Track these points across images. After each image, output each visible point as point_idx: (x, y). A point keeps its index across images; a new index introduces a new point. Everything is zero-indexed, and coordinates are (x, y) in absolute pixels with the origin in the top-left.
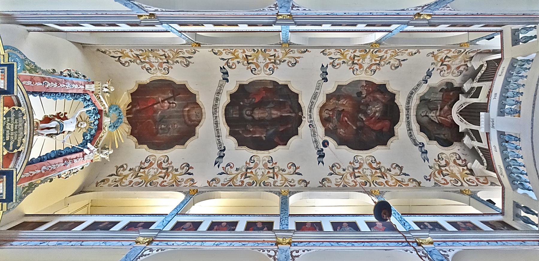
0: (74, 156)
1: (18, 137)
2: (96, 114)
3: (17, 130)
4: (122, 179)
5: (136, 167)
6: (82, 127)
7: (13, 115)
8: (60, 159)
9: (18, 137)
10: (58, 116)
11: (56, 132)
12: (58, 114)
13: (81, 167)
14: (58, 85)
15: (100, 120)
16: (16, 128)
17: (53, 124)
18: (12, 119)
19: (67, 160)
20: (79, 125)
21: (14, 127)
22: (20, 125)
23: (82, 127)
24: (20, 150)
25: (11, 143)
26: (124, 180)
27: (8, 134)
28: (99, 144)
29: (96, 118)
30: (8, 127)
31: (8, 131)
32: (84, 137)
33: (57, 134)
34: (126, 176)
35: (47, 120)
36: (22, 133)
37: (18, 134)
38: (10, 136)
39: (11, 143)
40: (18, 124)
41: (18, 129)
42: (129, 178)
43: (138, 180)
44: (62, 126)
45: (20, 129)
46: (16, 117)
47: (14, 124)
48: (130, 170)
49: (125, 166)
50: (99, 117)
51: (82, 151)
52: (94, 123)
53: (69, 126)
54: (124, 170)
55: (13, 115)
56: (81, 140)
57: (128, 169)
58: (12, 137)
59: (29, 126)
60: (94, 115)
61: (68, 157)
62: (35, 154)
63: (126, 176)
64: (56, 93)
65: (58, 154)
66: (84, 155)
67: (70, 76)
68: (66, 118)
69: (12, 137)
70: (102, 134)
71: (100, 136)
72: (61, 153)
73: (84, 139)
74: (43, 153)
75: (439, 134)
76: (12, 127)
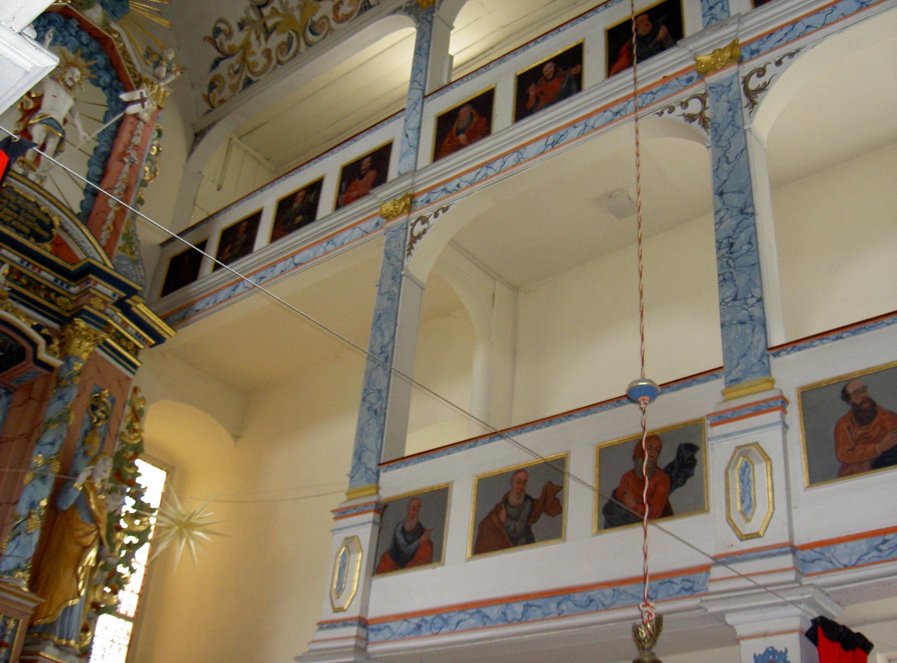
0: (125, 135)
1: (32, 214)
2: (66, 26)
3: (20, 208)
4: (244, 59)
5: (246, 12)
6: (76, 80)
8: (114, 164)
9: (32, 214)
11: (57, 140)
12: (22, 109)
13: (156, 134)
15: (84, 26)
16: (16, 208)
19: (124, 154)
20: (70, 83)
21: (10, 208)
22: (13, 198)
23: (76, 80)
24: (57, 224)
25: (38, 229)
26: (251, 59)
27: (20, 226)
28: (135, 69)
29: (73, 31)
30: (7, 219)
31: (14, 223)
32: (98, 85)
33: (62, 140)
34: (246, 47)
36: (29, 205)
37: (26, 211)
38: (23, 224)
39: (38, 229)
40: (9, 201)
41: (17, 205)
42: (258, 48)
43: (276, 39)
44: (50, 122)
45: (20, 202)
47: (7, 206)
48: (241, 26)
49: (223, 26)
50: (74, 23)
51: (125, 116)
52: (82, 44)
54: (229, 35)
56: (102, 97)
57: (235, 28)
58: (29, 223)
59: (23, 186)
60: (66, 33)
61: (120, 148)
62: (75, 199)
63: (246, 47)
66: (136, 116)
68: (38, 101)
69: (29, 223)
70: (118, 47)
71: (120, 52)
72: (104, 153)
73: (104, 89)
76: (10, 212)
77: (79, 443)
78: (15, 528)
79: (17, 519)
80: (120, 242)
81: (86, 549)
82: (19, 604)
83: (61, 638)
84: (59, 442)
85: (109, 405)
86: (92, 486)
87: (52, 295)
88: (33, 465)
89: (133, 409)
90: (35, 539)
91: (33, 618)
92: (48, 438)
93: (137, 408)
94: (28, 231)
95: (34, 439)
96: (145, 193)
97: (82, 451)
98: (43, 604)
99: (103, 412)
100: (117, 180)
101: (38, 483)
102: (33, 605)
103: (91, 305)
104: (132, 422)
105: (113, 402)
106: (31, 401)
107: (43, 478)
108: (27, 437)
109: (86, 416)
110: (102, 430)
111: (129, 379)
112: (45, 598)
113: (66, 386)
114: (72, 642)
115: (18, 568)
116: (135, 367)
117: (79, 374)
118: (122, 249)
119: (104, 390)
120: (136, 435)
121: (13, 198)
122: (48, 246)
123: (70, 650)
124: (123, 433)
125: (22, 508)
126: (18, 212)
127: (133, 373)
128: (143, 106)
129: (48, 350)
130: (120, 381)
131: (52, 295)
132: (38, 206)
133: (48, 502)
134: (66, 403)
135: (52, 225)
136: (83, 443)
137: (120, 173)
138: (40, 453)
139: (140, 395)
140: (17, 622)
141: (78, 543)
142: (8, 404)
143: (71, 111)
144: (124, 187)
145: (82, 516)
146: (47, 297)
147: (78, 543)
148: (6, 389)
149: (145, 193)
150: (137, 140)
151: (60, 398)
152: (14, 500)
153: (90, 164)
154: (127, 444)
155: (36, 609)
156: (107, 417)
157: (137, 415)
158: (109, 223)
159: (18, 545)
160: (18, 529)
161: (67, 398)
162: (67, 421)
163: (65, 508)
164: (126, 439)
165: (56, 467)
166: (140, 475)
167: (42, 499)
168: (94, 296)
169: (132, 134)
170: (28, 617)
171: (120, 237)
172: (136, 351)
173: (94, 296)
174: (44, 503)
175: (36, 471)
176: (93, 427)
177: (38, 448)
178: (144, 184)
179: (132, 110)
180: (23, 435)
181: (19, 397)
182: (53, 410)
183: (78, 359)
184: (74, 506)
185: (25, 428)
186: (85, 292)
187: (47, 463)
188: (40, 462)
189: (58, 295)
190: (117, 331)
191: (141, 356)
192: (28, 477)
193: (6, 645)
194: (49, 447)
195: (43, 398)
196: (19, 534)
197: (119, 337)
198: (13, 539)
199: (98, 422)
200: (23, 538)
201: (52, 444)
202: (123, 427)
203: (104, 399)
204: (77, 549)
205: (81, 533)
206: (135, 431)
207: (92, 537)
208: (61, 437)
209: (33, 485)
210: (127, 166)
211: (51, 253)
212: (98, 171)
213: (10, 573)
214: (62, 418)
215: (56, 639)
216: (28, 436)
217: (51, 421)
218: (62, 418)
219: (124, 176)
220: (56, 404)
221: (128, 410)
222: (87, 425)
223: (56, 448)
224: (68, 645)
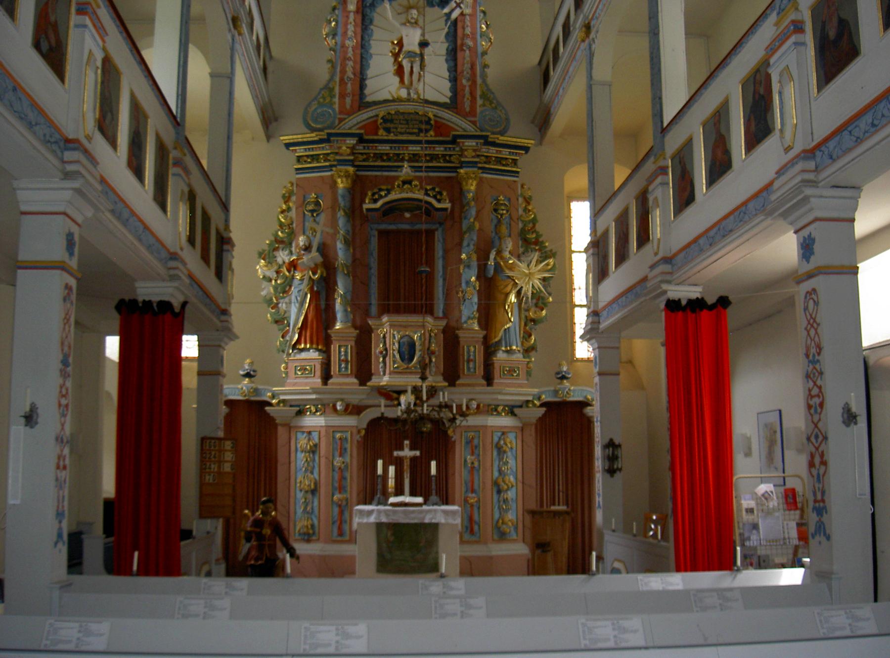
0: (460, 31)
3: (407, 120)
7: (388, 125)
10: (396, 56)
13: (482, 15)
14: (349, 59)
17: (406, 64)
18: (392, 126)
19: (462, 45)
20: (413, 21)
22: (401, 117)
24: (432, 117)
27: (411, 131)
30: (403, 130)
35: (400, 71)
36: (412, 116)
46: (391, 121)
53: (412, 39)
55: (388, 125)
61: (459, 42)
64: (362, 57)
65: (453, 54)
67: (334, 35)
68: (400, 44)
74: (446, 74)
75: (342, 96)
77: (494, 234)
80: (479, 102)
83: (506, 347)
87: (447, 158)
89: (525, 198)
94: (416, 131)
96: (488, 59)
100: (463, 64)
101: (466, 270)
103: (466, 157)
107: (469, 267)
111: (515, 181)
114: (514, 347)
116: (518, 172)
118: (484, 105)
121: (401, 117)
122: (432, 133)
126: (407, 124)
128: (461, 8)
129: (439, 201)
131: (447, 158)
132: (417, 113)
135: (430, 119)
136: (496, 233)
137: (464, 58)
140: (475, 347)
143: (423, 35)
144: (469, 66)
146: (445, 161)
149: (488, 59)
150: (468, 31)
153: (447, 61)
156: (507, 211)
157: (528, 201)
158: (467, 95)
163: (490, 276)
166: (541, 235)
168: (466, 150)
169: (464, 28)
171: (478, 98)
172: (515, 162)
173: (466, 150)
178: (485, 53)
179: (454, 15)
183: (469, 191)
186: (462, 150)
187: (469, 257)
189: (450, 156)
190: (496, 157)
191: (519, 163)
192: (462, 267)
197: (499, 160)
201: (468, 245)
202: (521, 211)
204: (503, 296)
208: (472, 240)
210: (467, 52)
211: (435, 136)
212: (452, 64)
213: (466, 322)
214: (470, 228)
215: (503, 349)
219: (468, 59)
221: (521, 200)
222: (495, 221)
224: (511, 350)
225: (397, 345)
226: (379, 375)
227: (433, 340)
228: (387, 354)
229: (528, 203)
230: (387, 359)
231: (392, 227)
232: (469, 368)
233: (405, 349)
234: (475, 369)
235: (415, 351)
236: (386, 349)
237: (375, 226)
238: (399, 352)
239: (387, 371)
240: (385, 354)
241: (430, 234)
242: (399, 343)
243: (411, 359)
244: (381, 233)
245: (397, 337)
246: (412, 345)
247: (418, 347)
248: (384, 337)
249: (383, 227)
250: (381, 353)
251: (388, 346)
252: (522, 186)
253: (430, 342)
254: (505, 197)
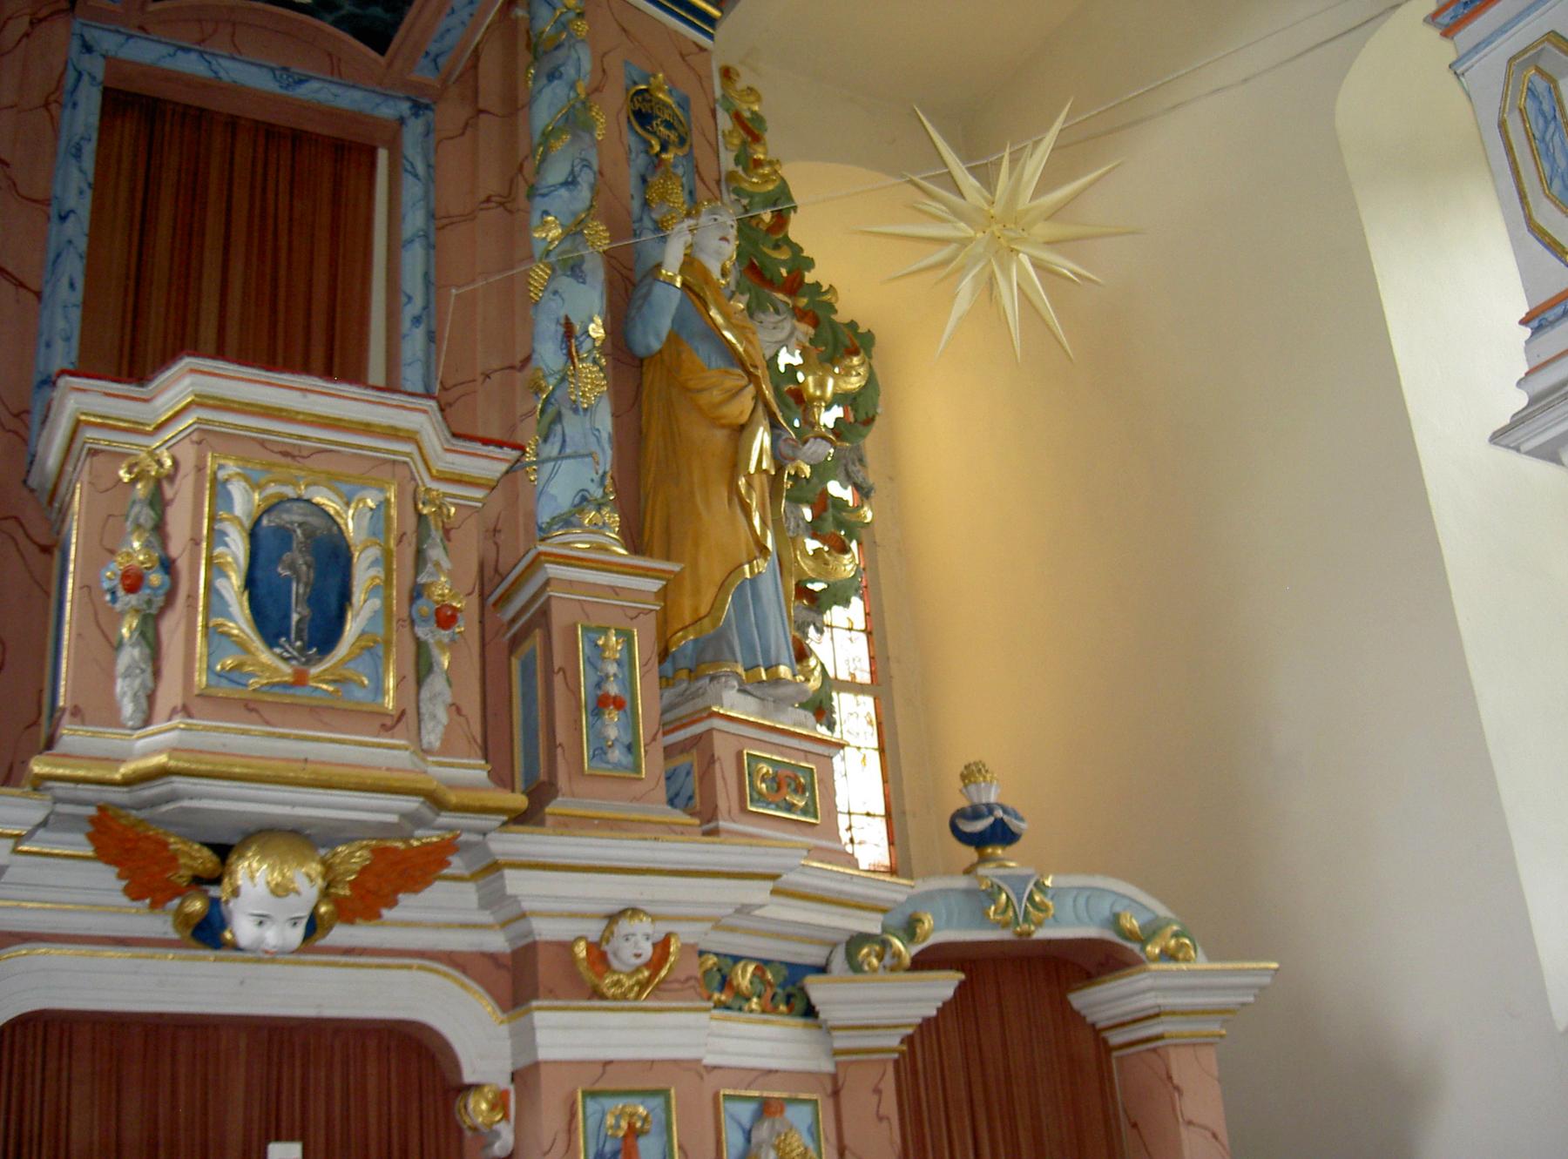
77: (636, 205)
78: (543, 411)
79: (538, 390)
81: (741, 432)
82: (615, 591)
84: (586, 178)
85: (678, 112)
86: (705, 274)
88: (539, 250)
89: (737, 117)
90: (605, 421)
91: (664, 620)
92: (556, 173)
93: (747, 114)
95: (522, 190)
97: (648, 223)
98: (677, 574)
99: (669, 125)
101: (565, 283)
102: (654, 585)
104: (744, 143)
105: (684, 104)
106: (482, 116)
107: (575, 269)
108: (501, 204)
109: (631, 140)
110: (680, 171)
111: (702, 49)
112: (679, 560)
113: (558, 47)
115: (583, 501)
116: (711, 21)
117: (580, 15)
119: (655, 76)
120: (766, 170)
123: (781, 691)
124: (731, 176)
125: (549, 355)
127: (711, 37)
130: (682, 56)
133: (604, 327)
134: (573, 86)
136: (646, 204)
138: (547, 213)
139: (741, 84)
141: (716, 422)
142: (427, 134)
145: (700, 356)
147: (716, 422)
148: (408, 99)
151: (553, 76)
152: (520, 357)
154: (751, 196)
155: (663, 594)
157: (751, 130)
159: (564, 441)
160: (551, 411)
161: (569, 71)
162: (589, 128)
163: (656, 346)
164: (745, 185)
165: (599, 237)
166: (809, 263)
167: (592, 321)
170: (651, 622)
174: (597, 330)
175: (552, 259)
176: (656, 163)
177: (540, 204)
180: (488, 200)
181: (452, 113)
182: (546, 107)
184: (674, 338)
185: (491, 184)
187: (574, 231)
188: (556, 232)
192: (540, 273)
193: (618, 704)
194: (563, 192)
195: (514, 106)
196: (558, 417)
198: (545, 440)
199: (664, 148)
200: (572, 426)
201: (571, 183)
202: (728, 161)
203: (661, 96)
204: (720, 436)
205: (716, 395)
206: (758, 164)
207: (746, 402)
209: (555, 293)
216: (506, 202)
217: (546, 136)
218: (575, 121)
220: (547, 94)
221: (725, 122)
222: (641, 161)
223: (584, 193)
224: (777, 681)
225: (236, 548)
226: (111, 717)
227: (436, 553)
228: (171, 596)
229: (757, 139)
230: (171, 627)
231: (190, 64)
232: (600, 752)
233: (295, 574)
234: (631, 748)
235: (345, 596)
236: (168, 566)
237: (108, 42)
238: (250, 583)
239: (170, 693)
240: (156, 591)
241: (347, 155)
242: (253, 535)
243: (325, 633)
244: (129, 105)
245: (243, 501)
246: (333, 557)
247: (364, 574)
248: (158, 502)
249: (145, 52)
250: (133, 581)
251: (177, 547)
252: (727, 73)
253: (420, 557)
254: (668, 79)
